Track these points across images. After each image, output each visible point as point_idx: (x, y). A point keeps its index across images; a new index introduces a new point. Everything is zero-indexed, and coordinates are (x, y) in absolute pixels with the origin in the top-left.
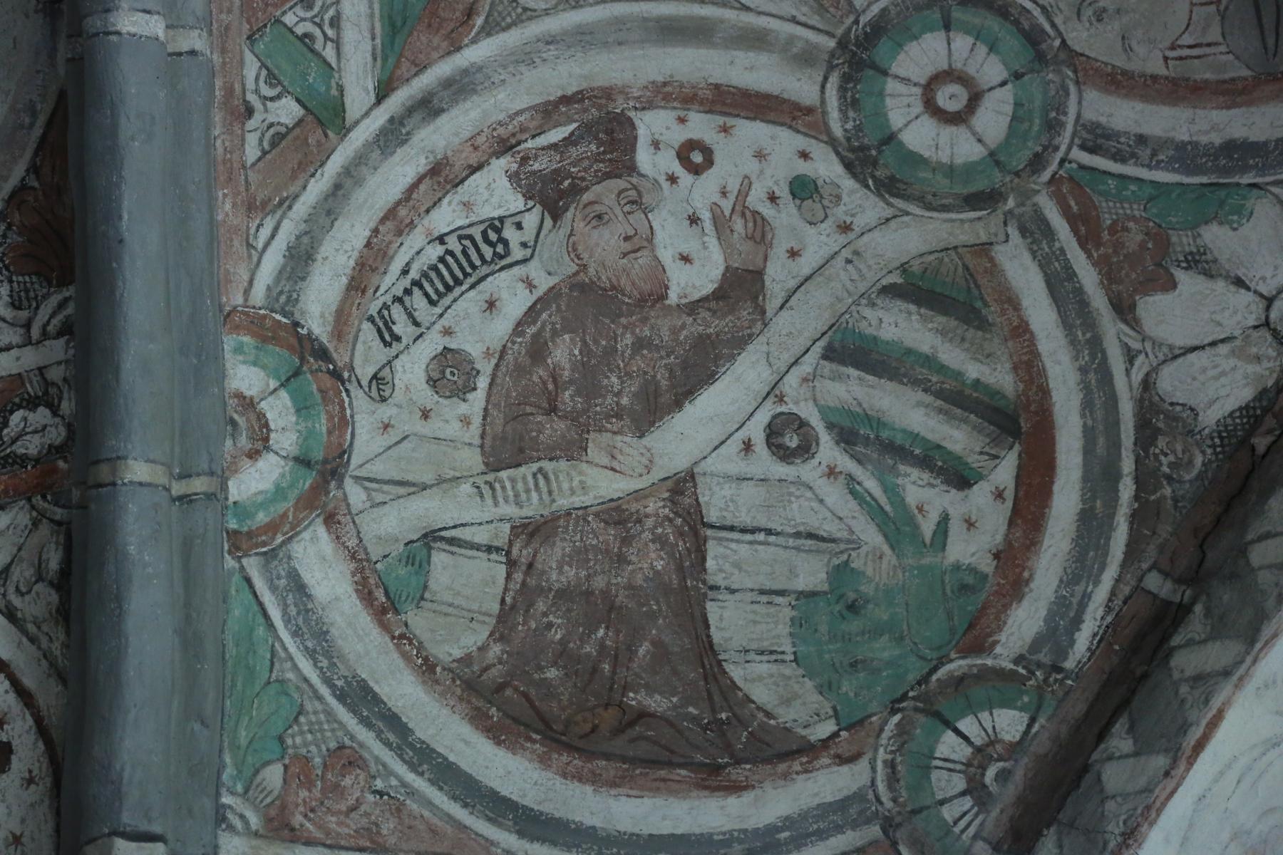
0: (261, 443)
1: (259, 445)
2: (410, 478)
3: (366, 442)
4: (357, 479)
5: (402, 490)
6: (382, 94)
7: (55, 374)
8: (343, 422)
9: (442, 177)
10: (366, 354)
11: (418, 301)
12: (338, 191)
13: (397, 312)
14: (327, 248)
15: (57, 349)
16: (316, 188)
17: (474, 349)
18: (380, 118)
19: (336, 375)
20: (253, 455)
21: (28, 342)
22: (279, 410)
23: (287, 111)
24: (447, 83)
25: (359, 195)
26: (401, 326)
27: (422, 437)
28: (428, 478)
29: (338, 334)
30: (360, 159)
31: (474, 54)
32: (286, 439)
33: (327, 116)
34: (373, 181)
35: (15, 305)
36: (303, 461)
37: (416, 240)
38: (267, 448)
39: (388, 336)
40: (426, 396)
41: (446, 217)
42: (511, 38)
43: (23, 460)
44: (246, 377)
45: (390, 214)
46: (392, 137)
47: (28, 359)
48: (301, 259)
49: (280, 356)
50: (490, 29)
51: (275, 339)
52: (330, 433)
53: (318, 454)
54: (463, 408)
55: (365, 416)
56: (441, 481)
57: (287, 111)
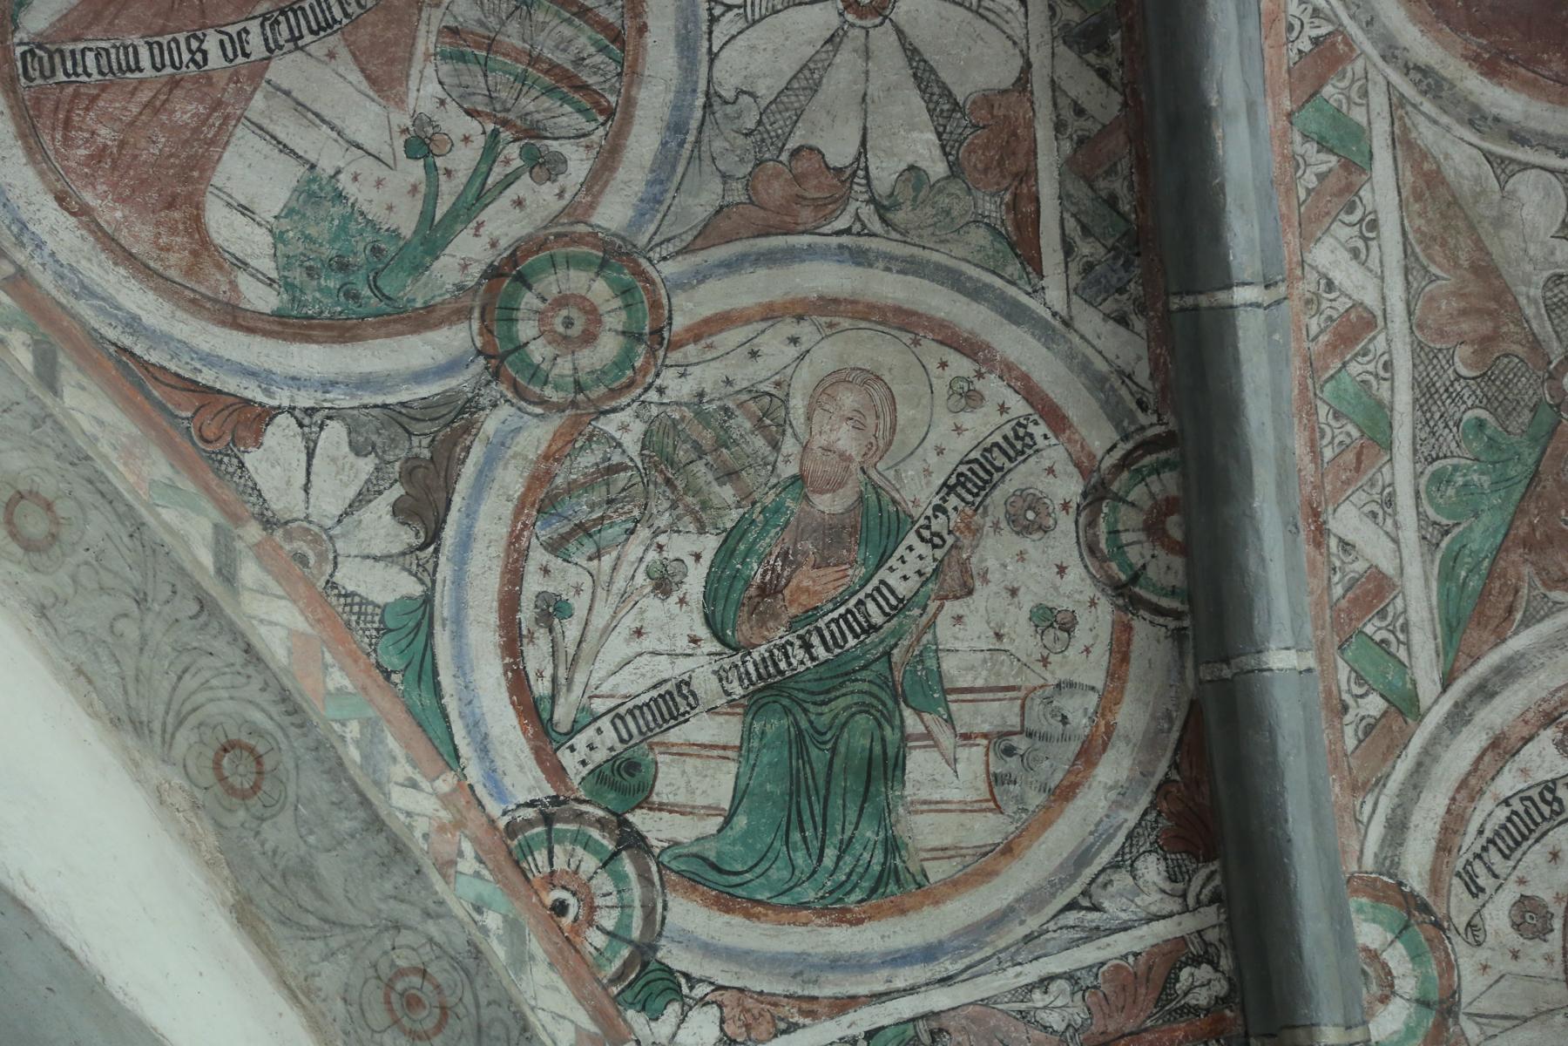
0: (1388, 992)
1: (1387, 991)
2: (1511, 1012)
3: (1471, 983)
4: (1469, 1015)
5: (1507, 1024)
6: (1446, 684)
7: (1212, 936)
8: (1449, 966)
9: (1502, 748)
10: (1459, 906)
11: (1494, 856)
12: (1421, 768)
13: (1478, 867)
14: (1416, 818)
15: (1210, 915)
16: (1403, 767)
17: (1547, 896)
18: (1446, 703)
19: (1437, 925)
20: (1384, 1000)
21: (1186, 910)
22: (1397, 958)
23: (1374, 705)
24: (1498, 670)
25: (1438, 770)
26: (1484, 880)
27: (1516, 976)
28: (1526, 1011)
29: (1435, 890)
30: (1434, 740)
31: (1518, 643)
32: (1407, 985)
33: (1405, 706)
34: (1447, 757)
35: (1172, 879)
36: (1423, 1002)
37: (1486, 804)
38: (1394, 993)
39: (1476, 890)
40: (1513, 939)
41: (1508, 782)
42: (1545, 628)
43: (1195, 1010)
44: (1369, 934)
45: (1463, 784)
46: (1458, 718)
47: (1189, 924)
48: (1398, 827)
49: (1391, 911)
50: (1526, 623)
51: (1386, 898)
52: (1441, 976)
53: (1434, 996)
54: (1545, 948)
55: (1467, 960)
56: (1538, 1014)
57: (1374, 705)
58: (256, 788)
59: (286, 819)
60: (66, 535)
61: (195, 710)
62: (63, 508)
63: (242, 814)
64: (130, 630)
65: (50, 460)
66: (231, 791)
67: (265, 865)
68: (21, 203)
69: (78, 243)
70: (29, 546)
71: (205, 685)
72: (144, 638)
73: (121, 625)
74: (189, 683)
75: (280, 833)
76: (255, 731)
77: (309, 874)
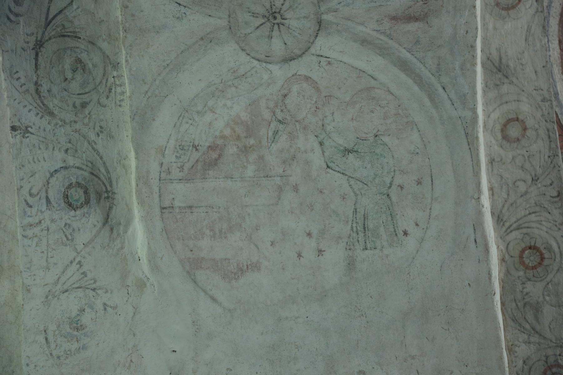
58: (534, 268)
59: (540, 285)
60: (524, 142)
61: (528, 228)
62: (529, 133)
63: (521, 273)
64: (522, 187)
65: (539, 114)
66: (522, 263)
67: (519, 296)
68: (551, 34)
69: (557, 58)
70: (505, 137)
71: (540, 222)
72: (526, 193)
73: (520, 183)
74: (533, 217)
75: (535, 290)
76: (549, 249)
77: (537, 309)
